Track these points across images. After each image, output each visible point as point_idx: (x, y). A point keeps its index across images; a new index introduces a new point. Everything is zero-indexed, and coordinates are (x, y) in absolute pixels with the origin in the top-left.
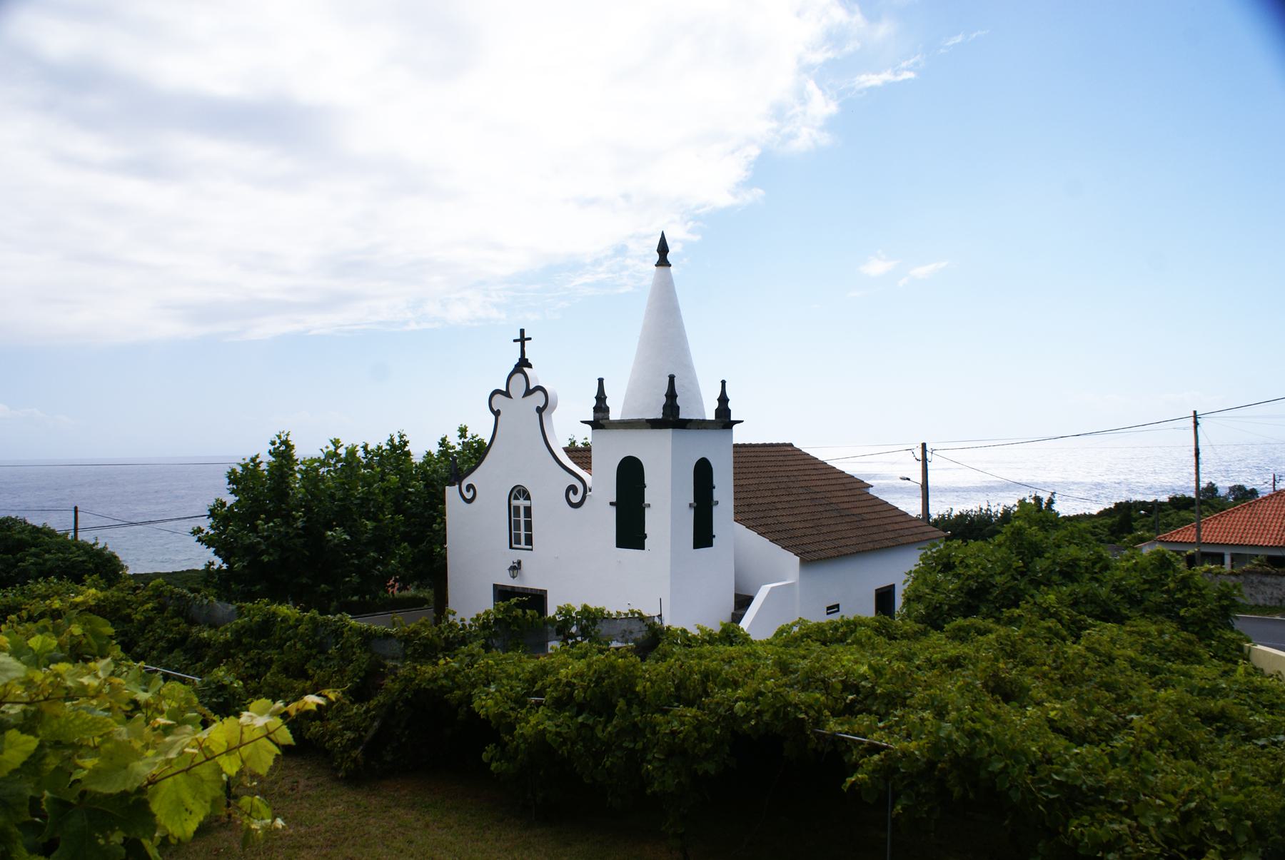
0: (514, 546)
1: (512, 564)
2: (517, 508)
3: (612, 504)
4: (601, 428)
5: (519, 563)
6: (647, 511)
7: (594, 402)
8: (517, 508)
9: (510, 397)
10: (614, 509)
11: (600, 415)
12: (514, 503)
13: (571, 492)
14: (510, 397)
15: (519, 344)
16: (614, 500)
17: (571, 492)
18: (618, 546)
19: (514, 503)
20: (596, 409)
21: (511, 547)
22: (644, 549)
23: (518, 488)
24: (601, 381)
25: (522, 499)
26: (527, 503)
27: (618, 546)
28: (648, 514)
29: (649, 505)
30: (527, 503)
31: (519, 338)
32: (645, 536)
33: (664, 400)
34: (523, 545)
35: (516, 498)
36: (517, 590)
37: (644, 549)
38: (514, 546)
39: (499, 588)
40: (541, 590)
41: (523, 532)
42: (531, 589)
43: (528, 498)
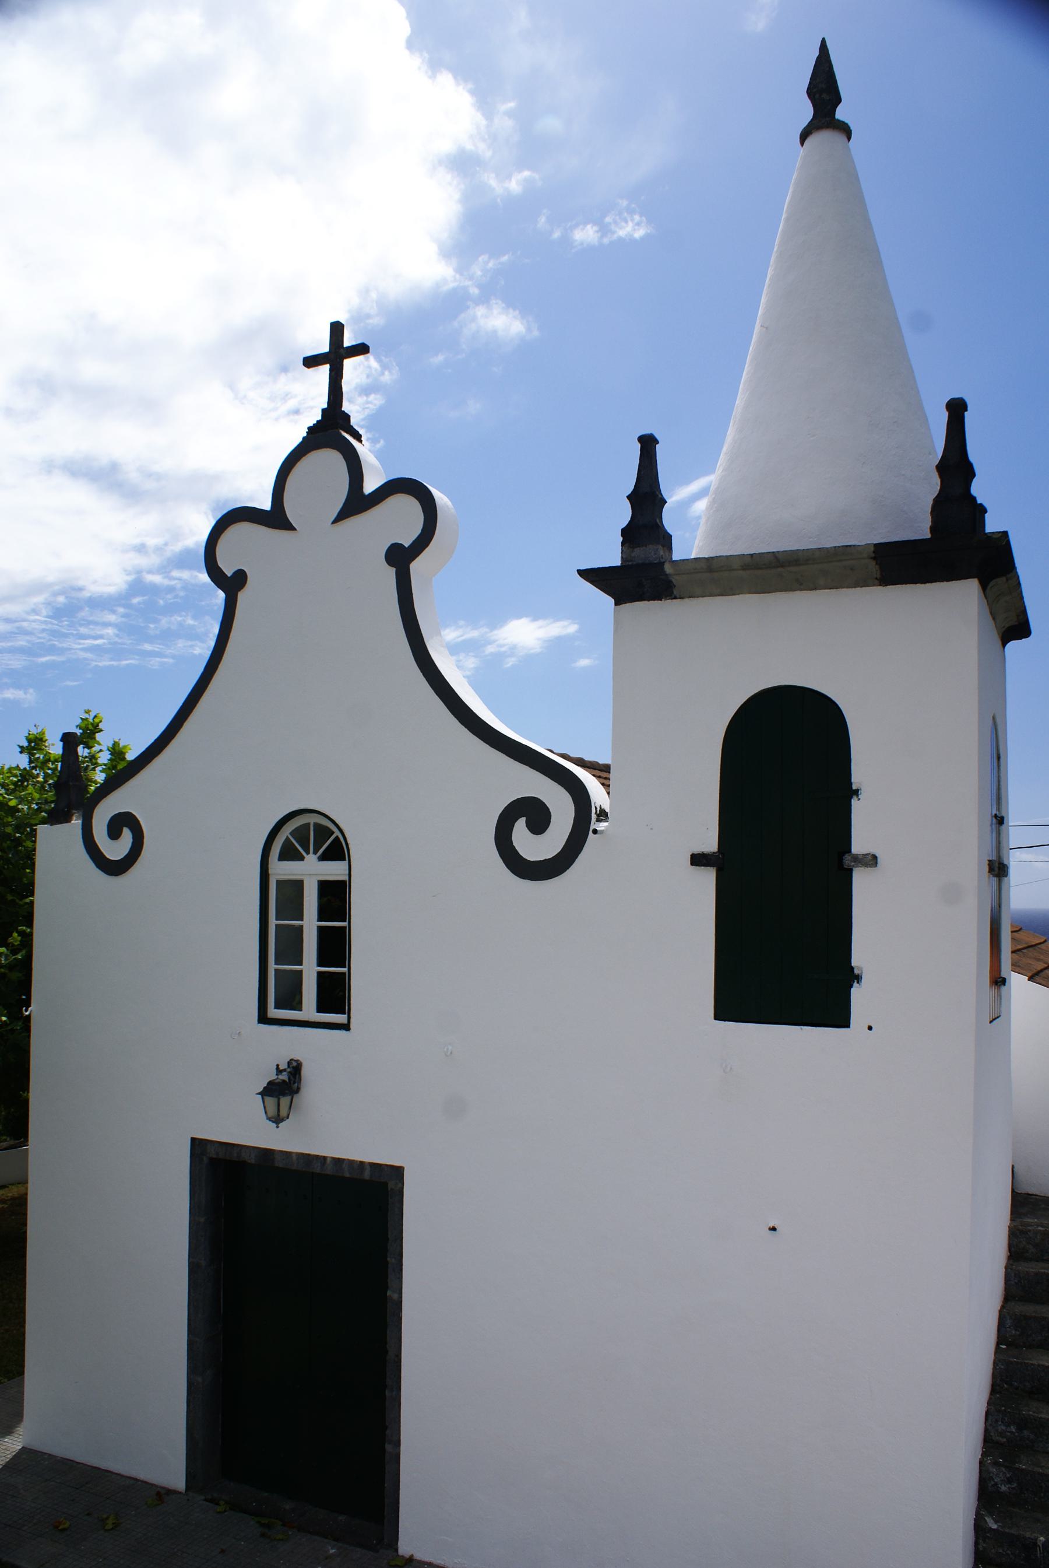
0: (273, 1012)
1: (273, 1076)
2: (293, 890)
3: (698, 860)
4: (657, 597)
5: (295, 1069)
6: (861, 881)
7: (624, 514)
8: (293, 890)
9: (289, 527)
10: (707, 879)
11: (608, 791)
12: (282, 870)
13: (521, 825)
14: (289, 527)
15: (324, 371)
16: (710, 844)
17: (521, 825)
18: (717, 1017)
19: (282, 870)
20: (630, 535)
21: (264, 1018)
22: (846, 1024)
23: (312, 819)
24: (648, 444)
25: (311, 859)
26: (334, 870)
27: (717, 1017)
28: (858, 808)
29: (871, 861)
30: (334, 870)
31: (325, 348)
32: (852, 977)
33: (934, 484)
34: (309, 1009)
35: (289, 854)
36: (279, 1163)
37: (846, 1024)
38: (273, 1012)
39: (212, 1152)
40: (375, 1167)
41: (310, 969)
42: (338, 1161)
43: (337, 851)
